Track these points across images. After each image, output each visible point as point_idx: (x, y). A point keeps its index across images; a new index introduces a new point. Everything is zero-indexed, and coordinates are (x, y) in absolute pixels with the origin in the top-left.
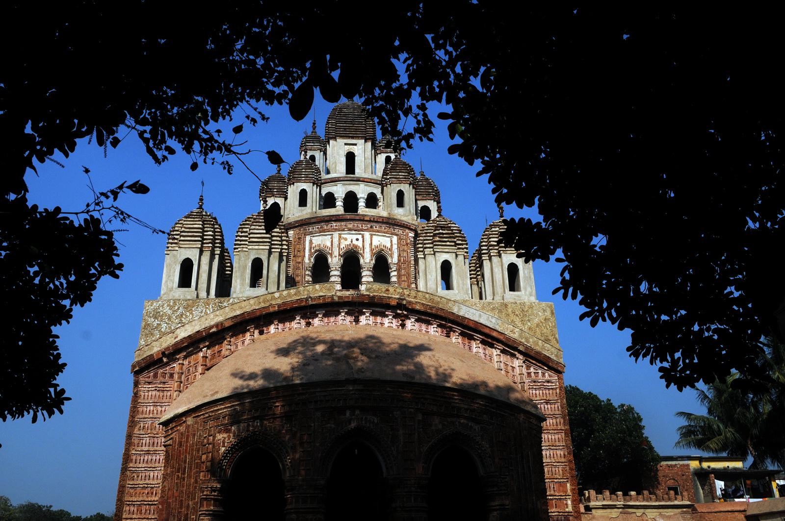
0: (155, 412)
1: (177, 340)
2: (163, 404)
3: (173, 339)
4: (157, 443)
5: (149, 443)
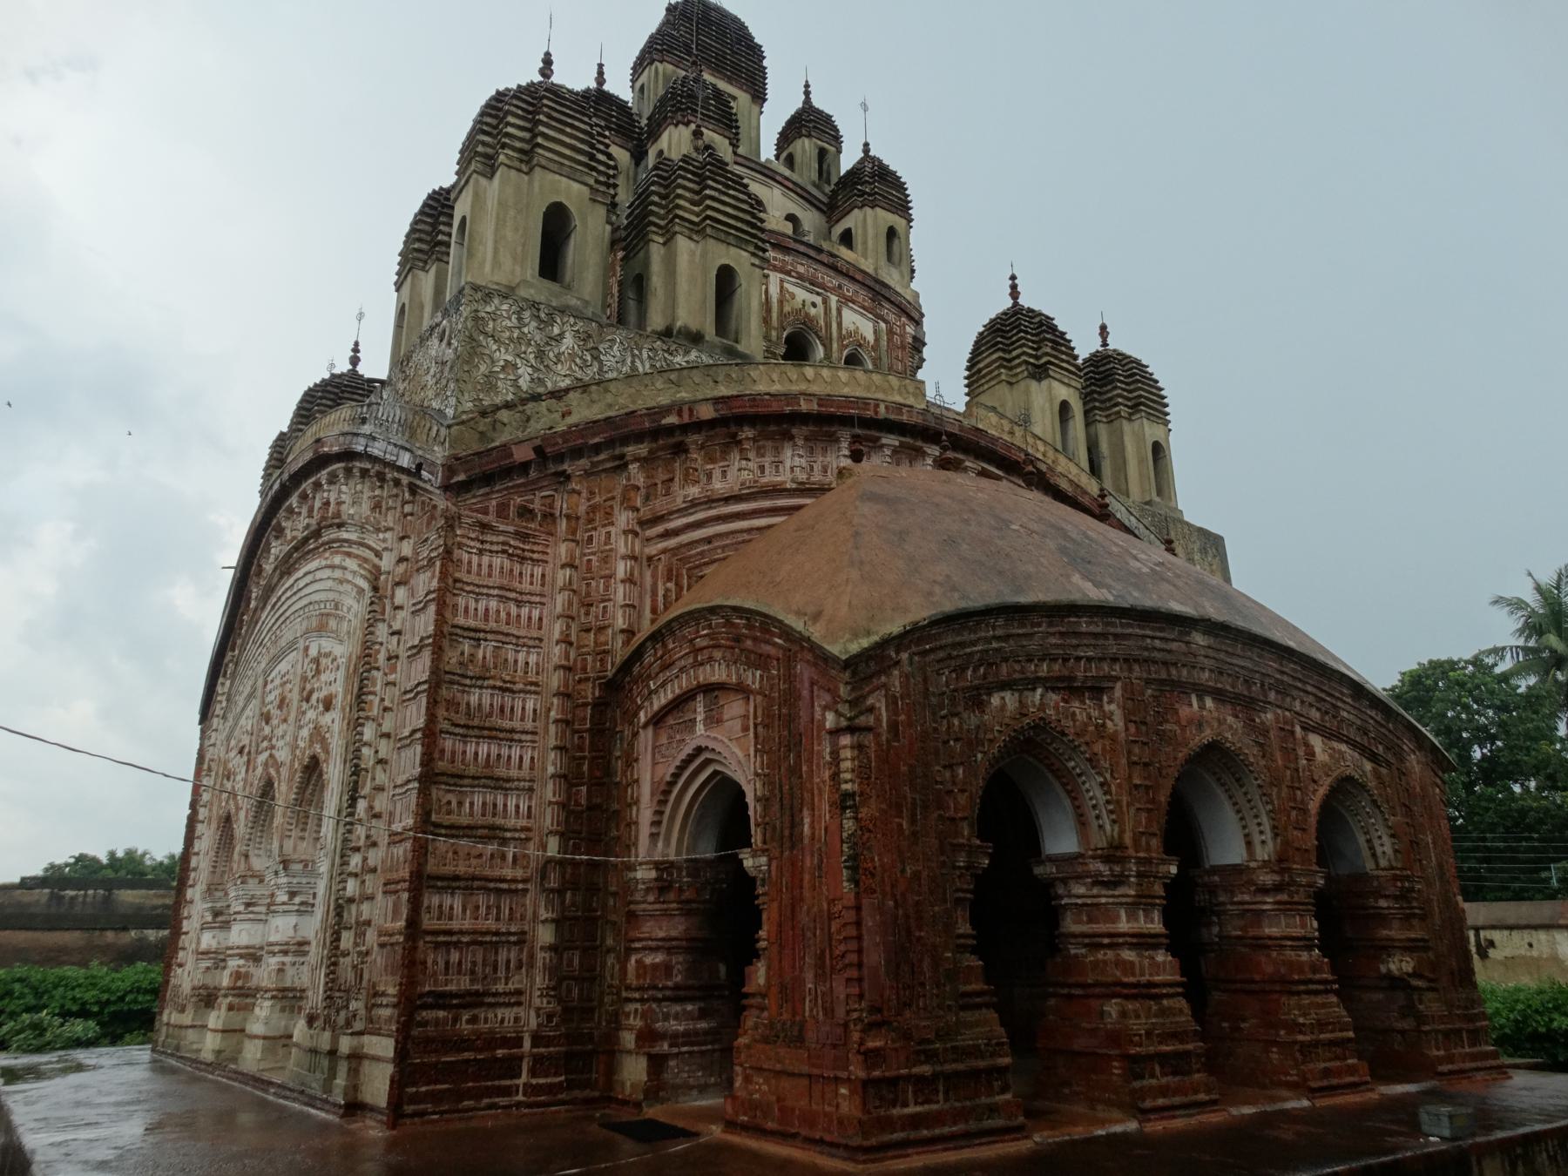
0: (503, 615)
1: (570, 420)
2: (525, 598)
3: (557, 416)
4: (512, 708)
5: (492, 705)
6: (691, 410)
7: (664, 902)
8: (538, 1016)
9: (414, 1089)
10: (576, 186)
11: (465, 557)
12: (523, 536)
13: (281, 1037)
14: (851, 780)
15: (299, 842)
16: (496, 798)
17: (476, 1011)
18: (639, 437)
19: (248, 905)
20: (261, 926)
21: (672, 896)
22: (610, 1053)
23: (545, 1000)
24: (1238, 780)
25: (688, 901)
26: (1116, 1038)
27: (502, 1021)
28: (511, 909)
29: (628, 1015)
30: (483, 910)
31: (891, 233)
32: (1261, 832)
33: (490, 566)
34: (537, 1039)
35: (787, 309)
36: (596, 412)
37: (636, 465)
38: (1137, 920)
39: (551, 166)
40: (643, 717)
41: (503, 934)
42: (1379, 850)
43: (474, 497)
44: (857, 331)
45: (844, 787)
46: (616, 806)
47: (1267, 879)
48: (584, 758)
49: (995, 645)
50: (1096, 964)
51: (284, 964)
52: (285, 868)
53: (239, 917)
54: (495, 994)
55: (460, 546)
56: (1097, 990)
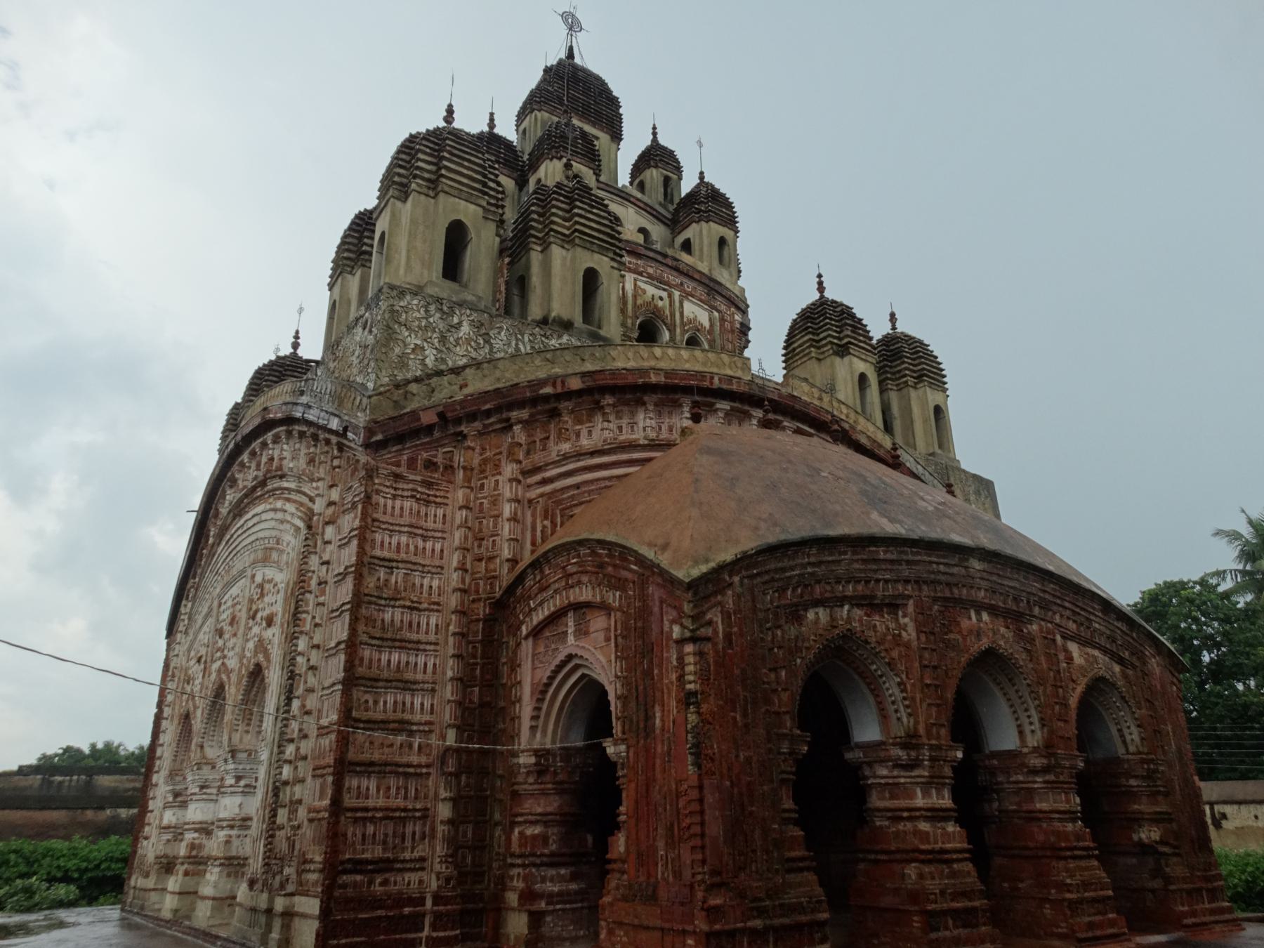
0: (412, 548)
1: (467, 391)
2: (430, 534)
3: (456, 388)
4: (419, 623)
5: (402, 621)
6: (563, 382)
7: (541, 783)
8: (438, 879)
9: (335, 942)
10: (472, 207)
11: (382, 501)
12: (429, 485)
13: (227, 898)
14: (694, 681)
15: (245, 735)
16: (404, 698)
17: (387, 875)
18: (521, 404)
19: (202, 787)
20: (211, 805)
21: (548, 778)
22: (498, 910)
23: (444, 866)
24: (1010, 680)
25: (561, 783)
26: (916, 896)
27: (409, 884)
28: (416, 789)
29: (512, 878)
30: (393, 791)
31: (722, 242)
32: (1031, 723)
33: (402, 508)
34: (437, 899)
35: (639, 302)
36: (487, 385)
37: (520, 426)
38: (930, 796)
39: (452, 192)
40: (524, 630)
41: (410, 810)
42: (1128, 738)
43: (390, 453)
44: (695, 319)
45: (689, 686)
46: (502, 704)
47: (1037, 762)
48: (476, 664)
49: (809, 570)
50: (897, 834)
51: (230, 836)
52: (233, 757)
53: (194, 797)
54: (404, 861)
55: (378, 492)
56: (898, 856)
